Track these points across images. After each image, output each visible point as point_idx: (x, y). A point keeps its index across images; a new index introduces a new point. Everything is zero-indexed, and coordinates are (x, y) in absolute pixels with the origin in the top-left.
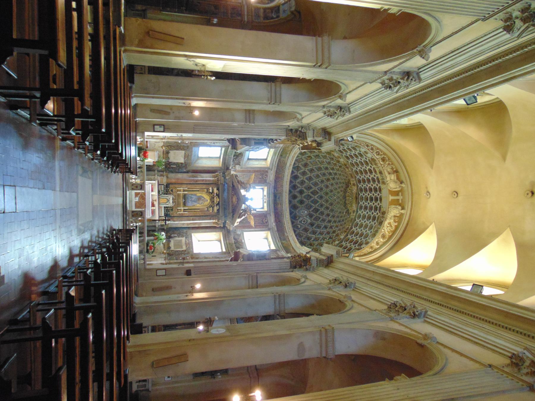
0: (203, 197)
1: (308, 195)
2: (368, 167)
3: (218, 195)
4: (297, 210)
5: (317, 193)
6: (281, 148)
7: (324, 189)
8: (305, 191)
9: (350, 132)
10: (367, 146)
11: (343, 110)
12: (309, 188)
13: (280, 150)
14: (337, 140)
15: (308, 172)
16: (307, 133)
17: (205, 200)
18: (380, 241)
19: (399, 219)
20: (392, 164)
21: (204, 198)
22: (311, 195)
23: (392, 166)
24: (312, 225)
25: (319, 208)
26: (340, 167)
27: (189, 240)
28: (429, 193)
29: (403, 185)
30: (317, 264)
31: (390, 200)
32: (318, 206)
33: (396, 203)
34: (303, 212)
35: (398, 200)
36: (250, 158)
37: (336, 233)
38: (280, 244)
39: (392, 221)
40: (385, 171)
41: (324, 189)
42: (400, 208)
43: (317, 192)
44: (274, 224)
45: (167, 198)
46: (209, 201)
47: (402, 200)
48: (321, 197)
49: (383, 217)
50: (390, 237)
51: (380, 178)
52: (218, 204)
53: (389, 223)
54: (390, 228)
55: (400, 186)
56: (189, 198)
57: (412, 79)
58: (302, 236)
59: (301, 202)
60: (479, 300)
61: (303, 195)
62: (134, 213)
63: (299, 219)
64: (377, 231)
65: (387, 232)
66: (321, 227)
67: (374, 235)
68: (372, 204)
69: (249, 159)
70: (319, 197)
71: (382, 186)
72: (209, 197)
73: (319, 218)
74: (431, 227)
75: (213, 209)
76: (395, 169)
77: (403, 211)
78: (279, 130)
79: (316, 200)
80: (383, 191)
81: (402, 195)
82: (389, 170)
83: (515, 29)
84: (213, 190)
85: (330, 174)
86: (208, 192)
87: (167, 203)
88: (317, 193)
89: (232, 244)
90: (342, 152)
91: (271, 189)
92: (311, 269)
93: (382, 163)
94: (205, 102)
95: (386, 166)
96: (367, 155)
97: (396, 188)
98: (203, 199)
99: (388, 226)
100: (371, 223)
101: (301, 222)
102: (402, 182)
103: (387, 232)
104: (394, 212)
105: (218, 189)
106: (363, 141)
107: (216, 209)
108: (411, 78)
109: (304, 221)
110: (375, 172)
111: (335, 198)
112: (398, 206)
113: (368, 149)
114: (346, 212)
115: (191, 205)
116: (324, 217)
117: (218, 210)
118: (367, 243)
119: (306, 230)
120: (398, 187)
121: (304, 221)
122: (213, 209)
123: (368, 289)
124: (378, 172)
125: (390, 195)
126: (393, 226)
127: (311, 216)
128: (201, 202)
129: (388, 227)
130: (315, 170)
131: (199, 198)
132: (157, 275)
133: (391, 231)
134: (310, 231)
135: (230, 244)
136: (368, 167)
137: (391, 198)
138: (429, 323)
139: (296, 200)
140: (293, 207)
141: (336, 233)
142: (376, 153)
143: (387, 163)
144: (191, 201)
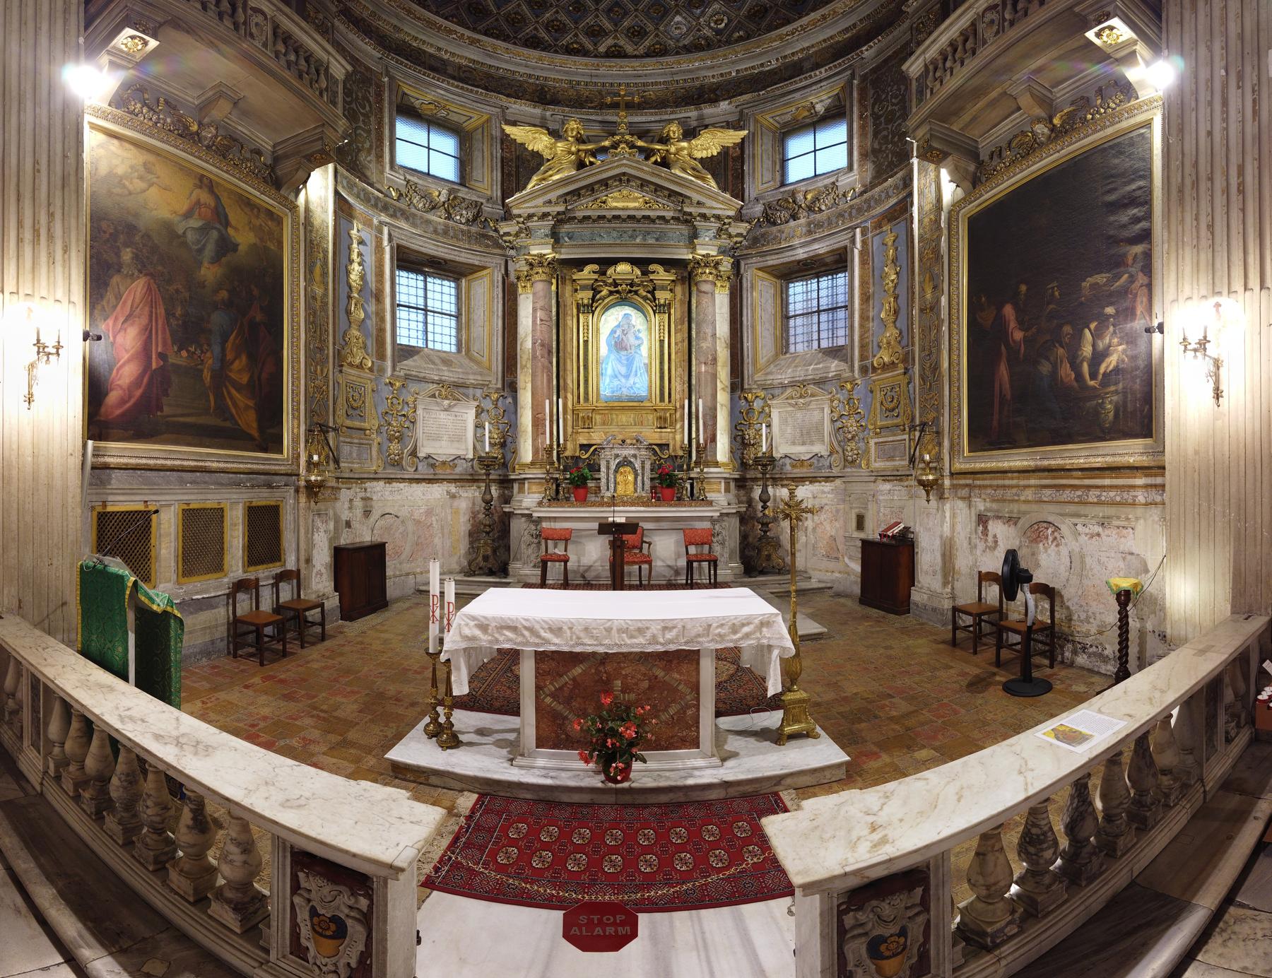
0: (613, 332)
21: (618, 326)
27: (784, 387)
45: (613, 467)
46: (628, 310)
56: (616, 383)
72: (612, 311)
86: (589, 308)
87: (638, 465)
98: (619, 332)
105: (580, 264)
107: (661, 275)
115: (645, 378)
117: (668, 264)
128: (632, 340)
131: (619, 345)
140: (659, 52)
144: (627, 377)
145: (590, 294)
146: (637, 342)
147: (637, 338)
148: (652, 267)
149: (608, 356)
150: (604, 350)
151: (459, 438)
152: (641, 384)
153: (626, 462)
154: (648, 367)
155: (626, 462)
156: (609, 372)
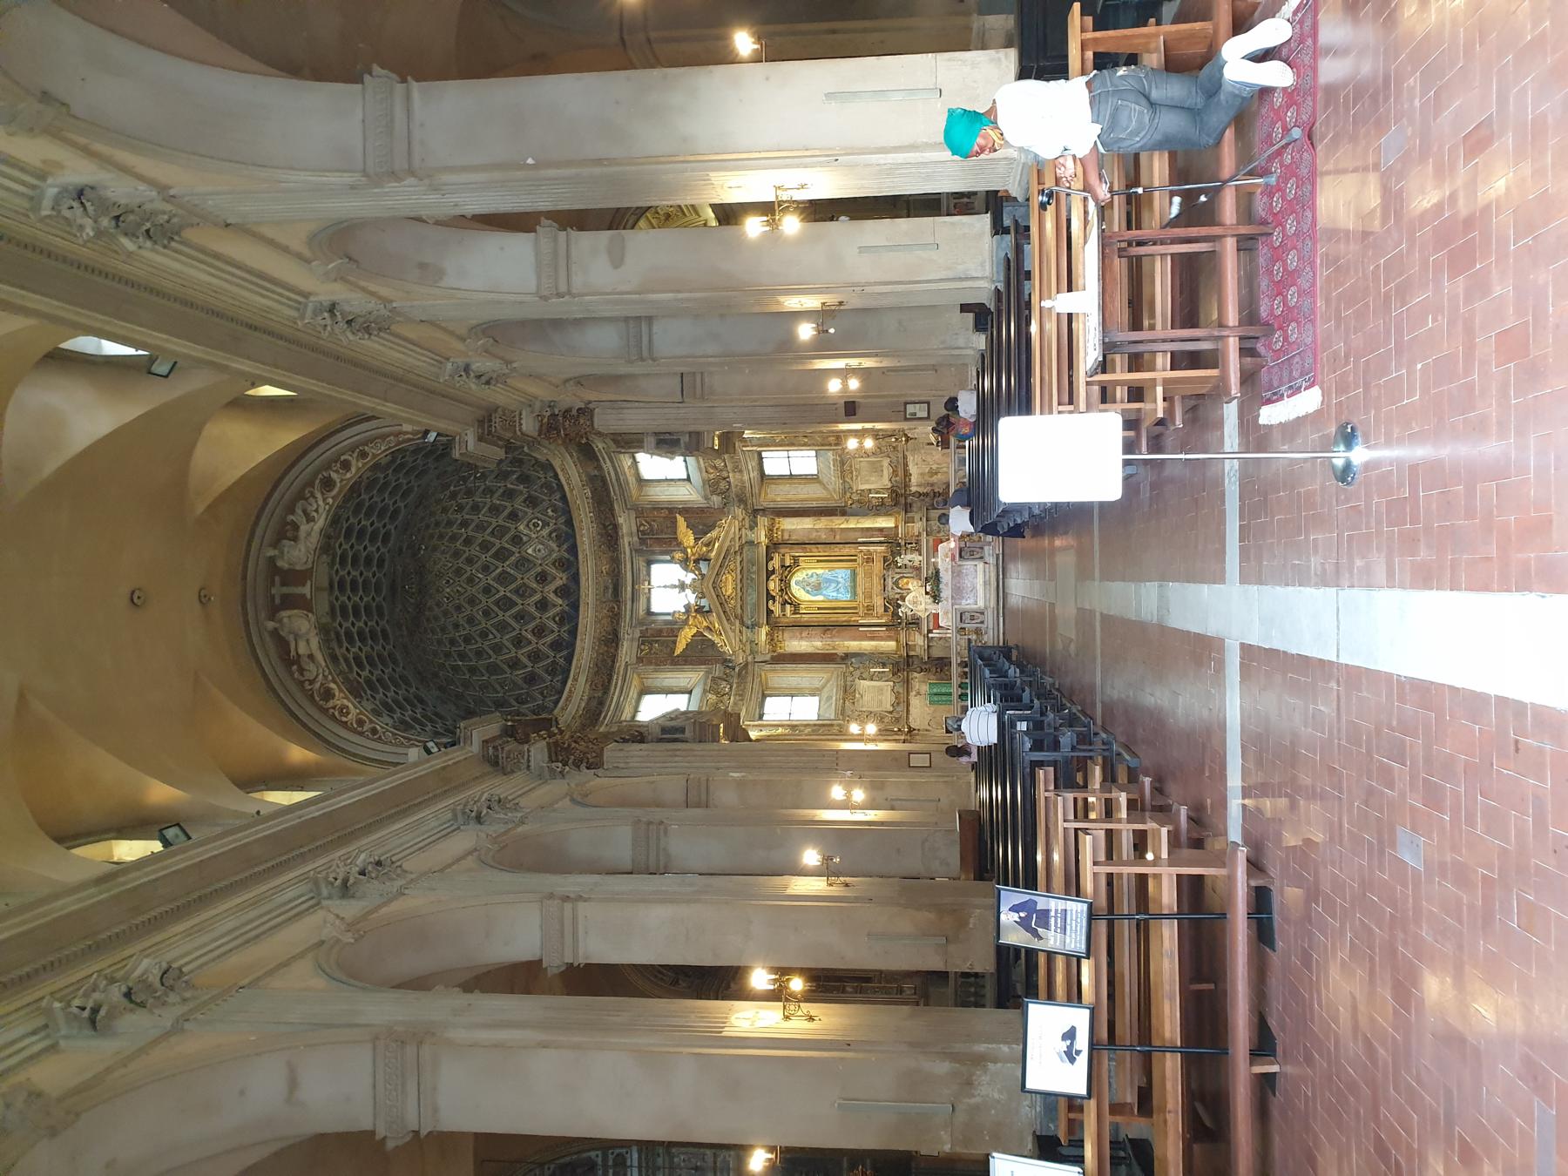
0: (808, 592)
1: (522, 596)
2: (365, 673)
3: (770, 597)
4: (554, 556)
5: (497, 603)
6: (603, 723)
7: (479, 616)
8: (532, 610)
9: (437, 763)
10: (374, 731)
11: (473, 814)
12: (522, 618)
13: (605, 718)
14: (465, 743)
15: (525, 660)
16: (547, 759)
17: (803, 584)
18: (337, 472)
19: (287, 532)
20: (303, 682)
22: (514, 598)
23: (303, 679)
24: (514, 516)
25: (492, 560)
26: (436, 675)
27: (844, 482)
28: (201, 601)
29: (271, 625)
30: (521, 419)
31: (309, 583)
32: (497, 567)
33: (294, 577)
34: (539, 550)
35: (283, 584)
36: (687, 696)
37: (448, 493)
38: (607, 466)
39: (304, 528)
40: (324, 664)
41: (479, 616)
42: (280, 563)
43: (499, 607)
44: (621, 520)
47: (273, 583)
48: (487, 590)
49: (329, 537)
50: (310, 484)
51: (335, 645)
52: (769, 574)
53: (310, 519)
54: (309, 508)
55: (280, 621)
56: (842, 590)
57: (336, 879)
58: (542, 487)
59: (543, 578)
60: (167, 340)
61: (537, 597)
62: (978, 556)
63: (551, 533)
64: (346, 500)
65: (319, 495)
66: (490, 510)
67: (354, 489)
68: (354, 573)
69: (690, 693)
70: (494, 591)
71: (326, 620)
72: (793, 592)
73: (492, 532)
74: (200, 508)
75: (783, 560)
76: (295, 667)
77: (271, 552)
78: (621, 765)
79: (501, 584)
80: (326, 608)
81: (273, 597)
82: (312, 667)
83: (155, 972)
84: (783, 610)
85: (462, 656)
86: (796, 607)
88: (497, 603)
89: (734, 471)
90: (436, 714)
91: (628, 613)
92: (538, 405)
93: (333, 686)
94: (817, 819)
95: (321, 676)
96: (374, 706)
97: (289, 617)
98: (808, 588)
99: (315, 514)
100: (380, 525)
101: (546, 524)
102: (275, 633)
103: (319, 495)
104: (299, 554)
105: (769, 612)
106: (386, 743)
107: (776, 563)
108: (338, 882)
109: (536, 525)
110: (346, 660)
111: (448, 590)
112: (286, 566)
113: (371, 721)
114: (420, 549)
116: (480, 537)
117: (769, 558)
118: (376, 467)
119: (532, 502)
120: (285, 620)
121: (536, 525)
122: (783, 560)
123: (410, 360)
124: (342, 660)
125: (309, 597)
126: (301, 513)
127: (517, 540)
129: (316, 511)
130: (505, 667)
131: (817, 588)
132: (928, 403)
133: (306, 499)
134: (522, 498)
135: (741, 471)
136: (365, 673)
137: (306, 590)
138: (301, 293)
139: (559, 583)
141: (448, 493)
142: (348, 713)
143: (317, 685)
144: (838, 583)
145: (788, 606)
146: (815, 576)
147: (812, 576)
148: (770, 568)
149: (824, 595)
150: (821, 598)
151: (881, 690)
152: (842, 574)
153: (896, 583)
154: (831, 569)
155: (896, 583)
156: (835, 594)
